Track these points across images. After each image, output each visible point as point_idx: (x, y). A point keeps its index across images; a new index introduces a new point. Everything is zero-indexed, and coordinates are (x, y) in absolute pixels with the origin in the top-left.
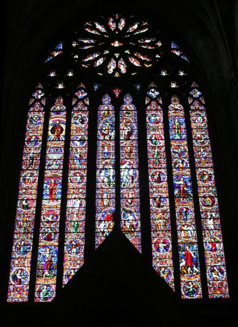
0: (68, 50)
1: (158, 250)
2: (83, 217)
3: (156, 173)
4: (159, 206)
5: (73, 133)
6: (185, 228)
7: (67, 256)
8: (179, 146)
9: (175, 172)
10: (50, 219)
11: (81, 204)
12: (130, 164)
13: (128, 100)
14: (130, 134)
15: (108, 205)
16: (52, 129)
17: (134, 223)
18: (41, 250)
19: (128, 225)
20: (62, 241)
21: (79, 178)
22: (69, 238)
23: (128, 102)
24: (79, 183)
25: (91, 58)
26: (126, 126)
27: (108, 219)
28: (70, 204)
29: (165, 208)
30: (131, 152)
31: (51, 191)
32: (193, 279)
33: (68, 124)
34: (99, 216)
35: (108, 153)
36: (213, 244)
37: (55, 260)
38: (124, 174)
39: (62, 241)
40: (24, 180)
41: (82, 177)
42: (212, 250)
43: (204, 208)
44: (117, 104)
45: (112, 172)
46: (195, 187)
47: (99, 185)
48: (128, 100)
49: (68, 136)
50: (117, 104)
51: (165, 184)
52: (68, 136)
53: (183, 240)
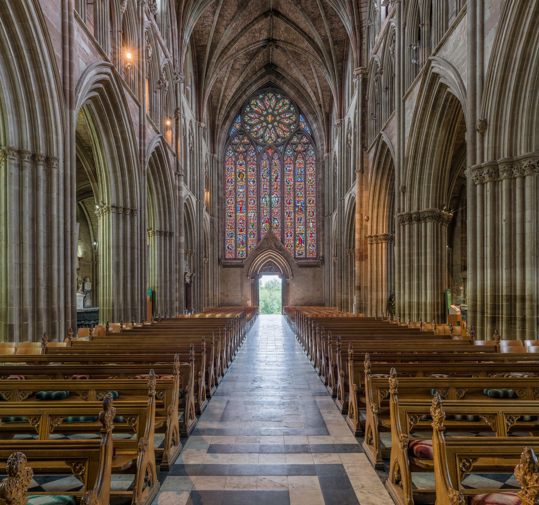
0: (243, 123)
1: (287, 236)
2: (256, 221)
3: (288, 199)
4: (289, 216)
5: (249, 177)
6: (300, 227)
7: (249, 239)
8: (300, 185)
9: (297, 199)
10: (241, 222)
11: (254, 215)
12: (276, 195)
13: (276, 156)
14: (277, 178)
15: (266, 216)
16: (239, 174)
17: (278, 224)
18: (238, 236)
19: (275, 225)
20: (247, 232)
21: (253, 202)
22: (250, 230)
23: (276, 159)
24: (253, 204)
25: (256, 129)
26: (275, 173)
27: (266, 222)
28: (249, 215)
29: (291, 217)
30: (277, 188)
31: (241, 208)
32: (301, 249)
33: (246, 172)
34: (262, 221)
35: (266, 189)
36: (311, 234)
37: (244, 241)
38: (273, 200)
39: (247, 232)
40: (228, 202)
41: (254, 202)
42: (310, 237)
43: (309, 217)
44: (271, 159)
45: (268, 199)
46: (306, 207)
47: (262, 206)
48: (276, 156)
49: (246, 179)
50: (271, 159)
51: (292, 205)
52: (246, 179)
53: (299, 232)
